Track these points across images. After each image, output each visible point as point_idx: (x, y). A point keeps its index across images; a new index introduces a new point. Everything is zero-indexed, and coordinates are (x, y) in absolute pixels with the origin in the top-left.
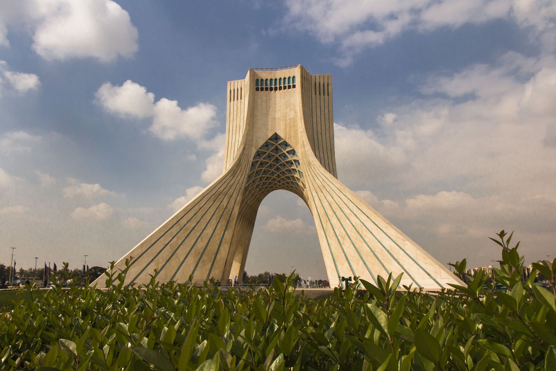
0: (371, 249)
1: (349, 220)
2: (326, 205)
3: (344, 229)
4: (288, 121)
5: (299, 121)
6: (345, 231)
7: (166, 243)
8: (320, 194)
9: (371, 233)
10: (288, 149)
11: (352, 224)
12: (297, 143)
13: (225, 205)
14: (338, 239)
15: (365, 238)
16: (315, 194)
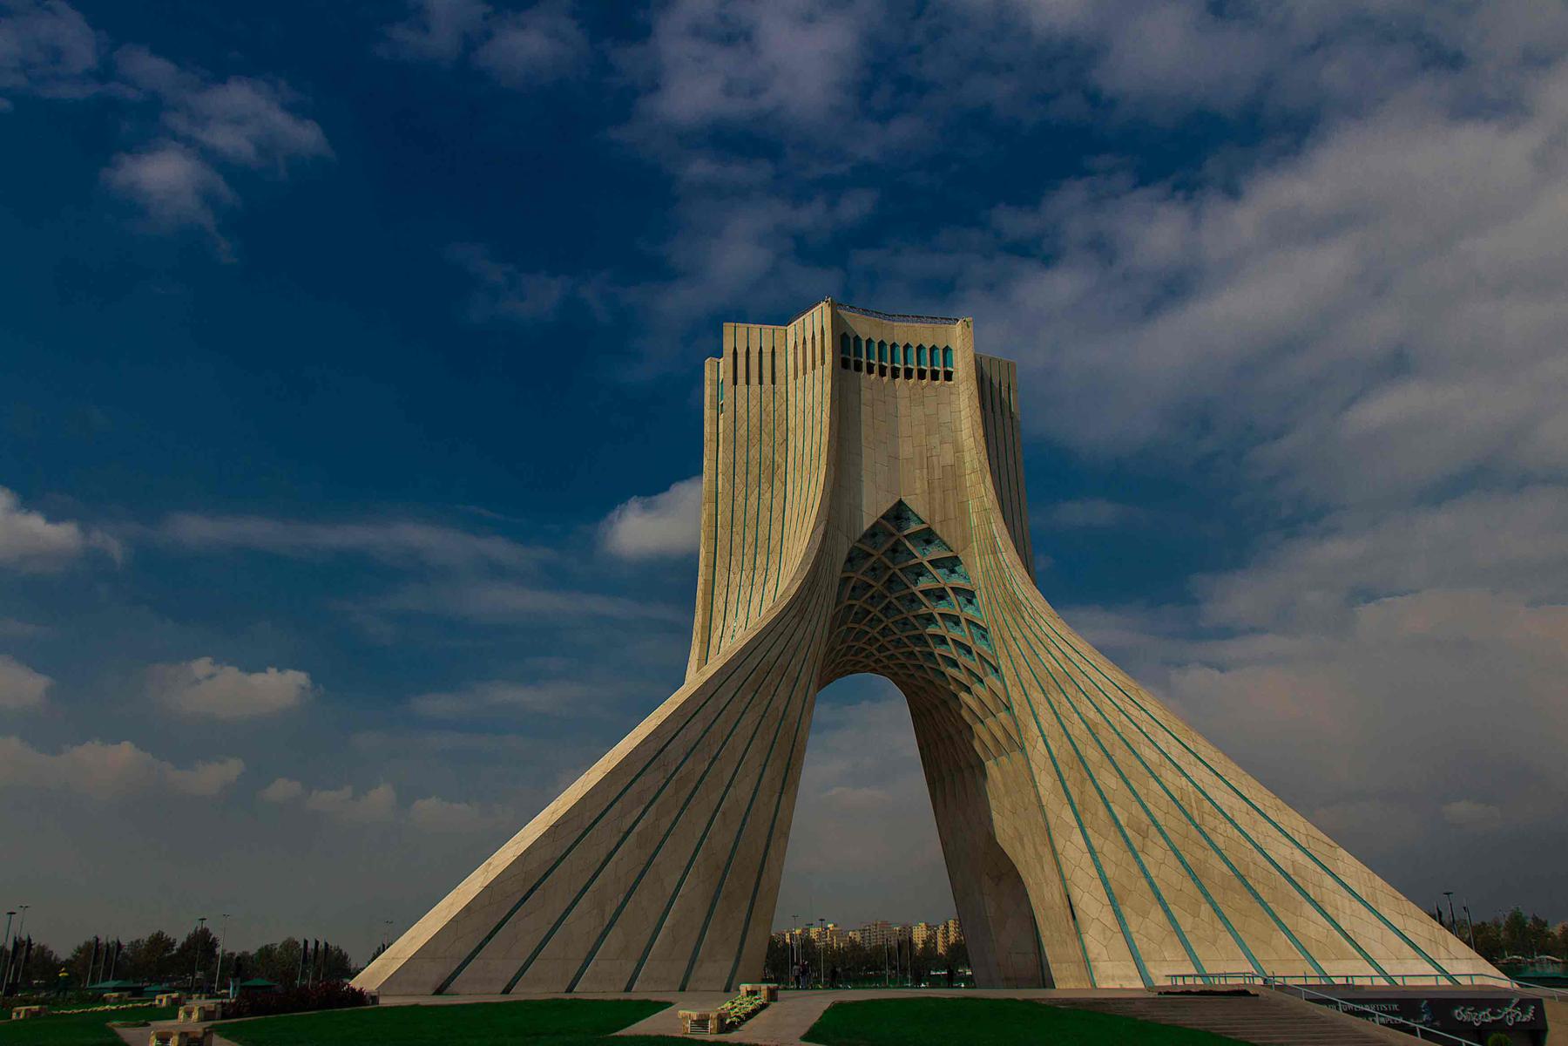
0: (1232, 868)
1: (1157, 780)
2: (1078, 729)
3: (1143, 806)
4: (937, 474)
5: (970, 479)
6: (1148, 813)
7: (626, 828)
8: (1055, 696)
9: (1231, 821)
10: (935, 552)
11: (1168, 792)
12: (967, 541)
13: (782, 708)
14: (1124, 836)
15: (1213, 837)
16: (1036, 695)
